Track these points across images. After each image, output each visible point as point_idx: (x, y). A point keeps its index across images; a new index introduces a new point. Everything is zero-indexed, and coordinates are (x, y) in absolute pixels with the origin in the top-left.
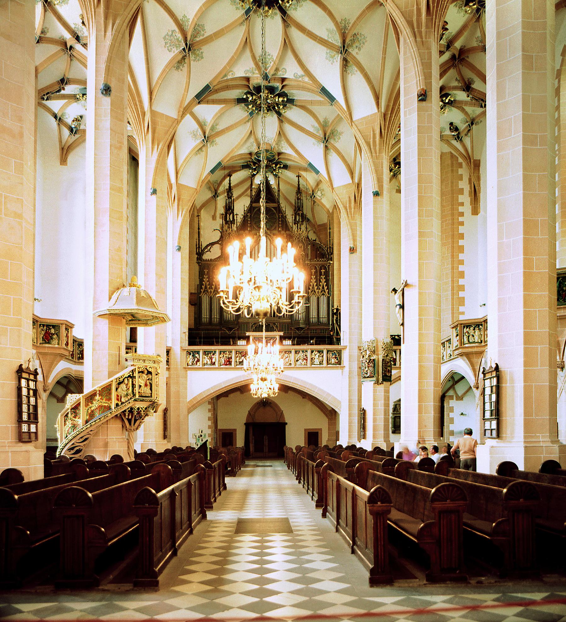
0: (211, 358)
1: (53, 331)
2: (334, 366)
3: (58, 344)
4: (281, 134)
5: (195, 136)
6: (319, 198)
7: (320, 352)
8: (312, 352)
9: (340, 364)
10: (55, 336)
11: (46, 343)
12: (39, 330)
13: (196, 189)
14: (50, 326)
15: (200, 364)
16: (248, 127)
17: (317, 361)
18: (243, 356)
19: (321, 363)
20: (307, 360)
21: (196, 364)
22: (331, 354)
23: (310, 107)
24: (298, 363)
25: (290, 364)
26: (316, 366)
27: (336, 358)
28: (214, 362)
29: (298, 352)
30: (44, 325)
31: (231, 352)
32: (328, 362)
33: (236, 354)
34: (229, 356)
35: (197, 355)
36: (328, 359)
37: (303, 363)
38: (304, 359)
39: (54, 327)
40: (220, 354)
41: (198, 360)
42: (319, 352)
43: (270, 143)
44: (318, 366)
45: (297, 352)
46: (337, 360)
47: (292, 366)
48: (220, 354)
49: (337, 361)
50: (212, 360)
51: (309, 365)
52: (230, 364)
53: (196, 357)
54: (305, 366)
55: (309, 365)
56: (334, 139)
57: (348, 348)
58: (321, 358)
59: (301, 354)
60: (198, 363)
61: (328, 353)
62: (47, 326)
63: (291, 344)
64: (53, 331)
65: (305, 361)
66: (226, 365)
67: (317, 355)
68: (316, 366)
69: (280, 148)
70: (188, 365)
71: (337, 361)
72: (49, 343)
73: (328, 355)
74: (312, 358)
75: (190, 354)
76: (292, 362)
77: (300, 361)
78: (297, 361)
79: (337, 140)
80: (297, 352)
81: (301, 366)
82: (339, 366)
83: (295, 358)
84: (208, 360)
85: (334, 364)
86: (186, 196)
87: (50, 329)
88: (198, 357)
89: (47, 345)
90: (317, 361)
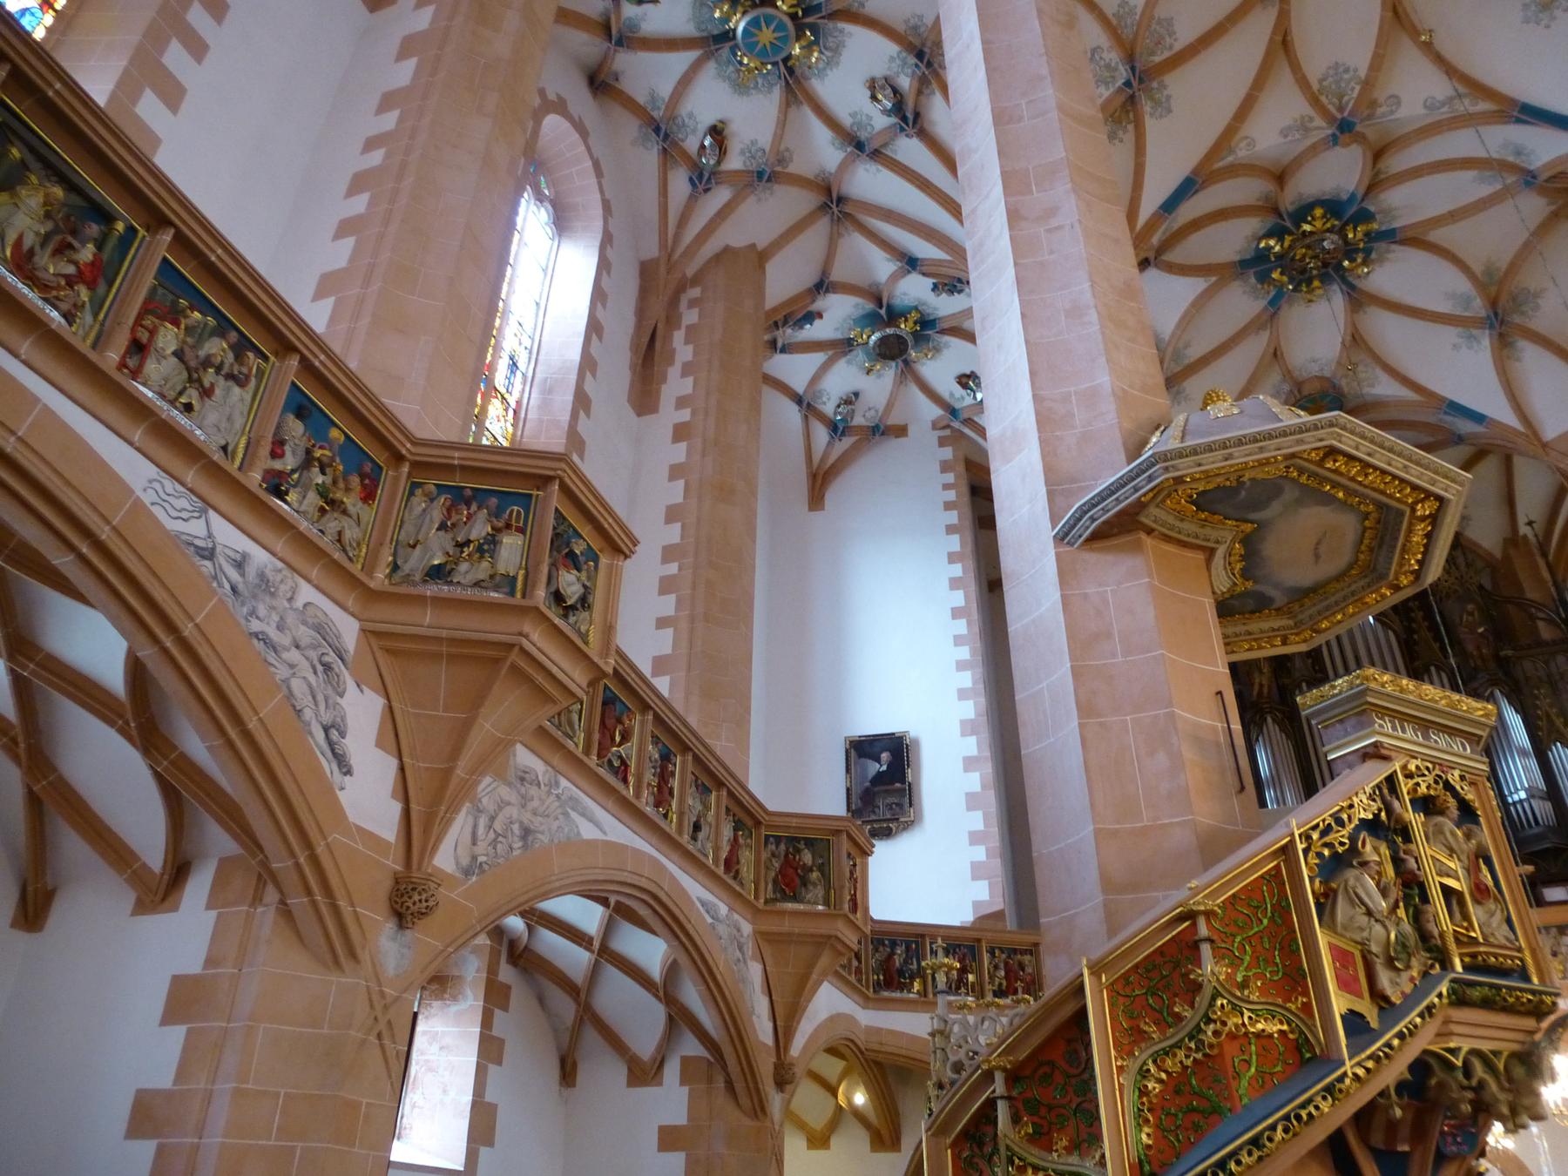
1: (807, 857)
3: (827, 903)
4: (1356, 340)
10: (815, 875)
11: (785, 898)
12: (765, 855)
14: (797, 840)
16: (1265, 336)
23: (1436, 236)
30: (778, 839)
39: (810, 843)
43: (1327, 374)
56: (1523, 313)
62: (793, 840)
64: (807, 857)
72: (795, 898)
79: (1530, 313)
87: (798, 851)
89: (790, 906)
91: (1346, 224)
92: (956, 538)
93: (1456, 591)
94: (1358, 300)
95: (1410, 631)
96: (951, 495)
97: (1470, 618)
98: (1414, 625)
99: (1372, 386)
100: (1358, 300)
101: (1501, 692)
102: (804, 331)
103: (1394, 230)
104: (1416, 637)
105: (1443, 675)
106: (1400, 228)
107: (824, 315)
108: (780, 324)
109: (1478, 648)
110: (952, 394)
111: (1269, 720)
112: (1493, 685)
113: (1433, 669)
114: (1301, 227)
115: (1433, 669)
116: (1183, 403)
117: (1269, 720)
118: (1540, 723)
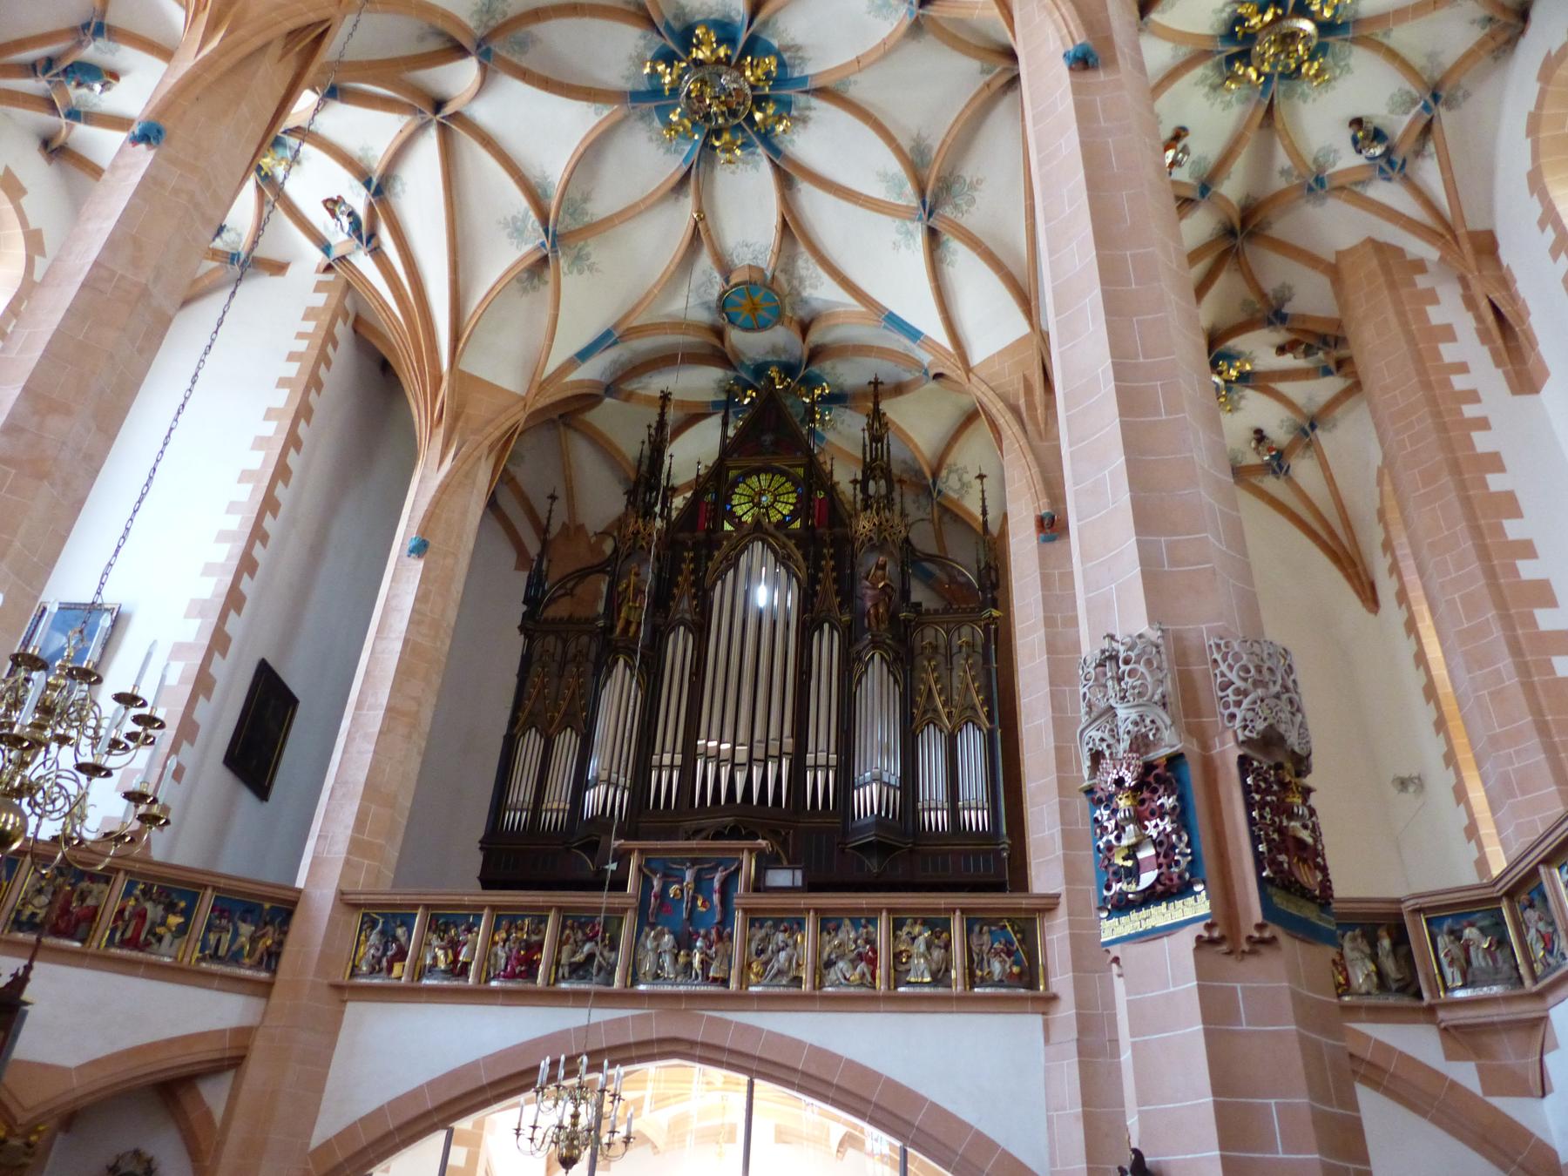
0: (454, 946)
2: (1003, 991)
4: (791, 229)
5: (517, 231)
6: (955, 496)
7: (937, 925)
8: (898, 925)
9: (1032, 984)
13: (523, 398)
15: (401, 973)
16: (686, 209)
17: (920, 970)
18: (590, 939)
19: (940, 976)
20: (873, 962)
21: (390, 969)
22: (986, 938)
24: (834, 974)
25: (797, 981)
26: (918, 990)
27: (1009, 954)
28: (466, 965)
29: (831, 925)
31: (544, 920)
32: (972, 974)
33: (564, 927)
34: (534, 938)
35: (400, 932)
36: (971, 960)
37: (855, 977)
38: (860, 954)
40: (497, 928)
41: (401, 955)
42: (926, 923)
44: (927, 990)
45: (828, 922)
46: (1015, 963)
47: (806, 987)
48: (497, 928)
49: (1016, 969)
50: (456, 955)
51: (881, 986)
52: (531, 973)
53: (395, 939)
54: (863, 990)
55: (881, 986)
57: (1063, 900)
58: (937, 954)
59: (848, 934)
60: (397, 968)
61: (970, 931)
63: (799, 882)
65: (862, 966)
66: (511, 976)
67: (920, 944)
68: (918, 990)
69: (796, 283)
70: (352, 975)
71: (1016, 969)
73: (975, 940)
74: (897, 956)
75: (374, 924)
76: (806, 975)
77: (841, 964)
78: (830, 964)
79: (965, 208)
80: (828, 922)
81: (843, 990)
82: (1030, 993)
83: (818, 952)
84: (440, 953)
85: (1000, 983)
86: (479, 409)
88: (403, 939)
90: (920, 970)
91: (742, 56)
92: (285, 393)
93: (871, 539)
94: (787, 175)
95: (813, 580)
96: (302, 346)
97: (880, 573)
98: (821, 575)
99: (816, 287)
100: (787, 175)
101: (882, 657)
102: (83, 91)
103: (806, 77)
104: (818, 588)
105: (836, 635)
106: (812, 76)
107: (122, 79)
108: (39, 69)
109: (876, 606)
110: (326, 228)
111: (621, 662)
112: (874, 648)
113: (826, 626)
114: (691, 53)
115: (826, 626)
116: (587, 273)
117: (621, 662)
118: (918, 699)
